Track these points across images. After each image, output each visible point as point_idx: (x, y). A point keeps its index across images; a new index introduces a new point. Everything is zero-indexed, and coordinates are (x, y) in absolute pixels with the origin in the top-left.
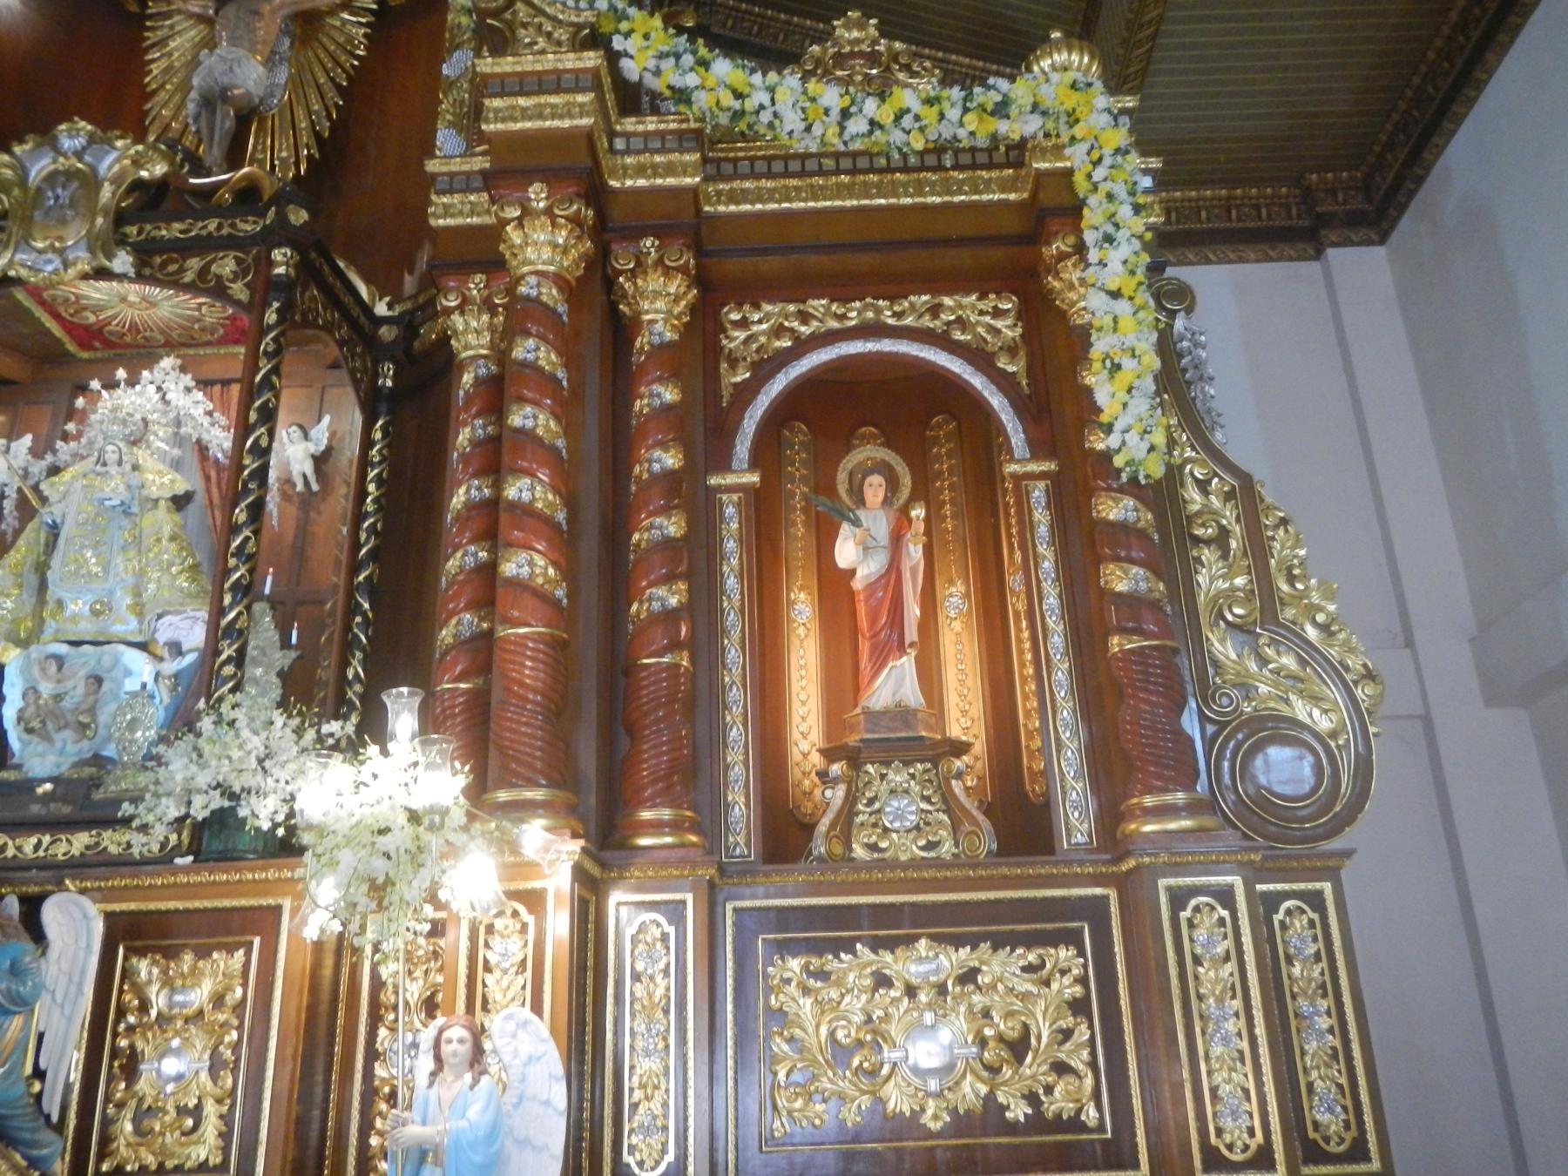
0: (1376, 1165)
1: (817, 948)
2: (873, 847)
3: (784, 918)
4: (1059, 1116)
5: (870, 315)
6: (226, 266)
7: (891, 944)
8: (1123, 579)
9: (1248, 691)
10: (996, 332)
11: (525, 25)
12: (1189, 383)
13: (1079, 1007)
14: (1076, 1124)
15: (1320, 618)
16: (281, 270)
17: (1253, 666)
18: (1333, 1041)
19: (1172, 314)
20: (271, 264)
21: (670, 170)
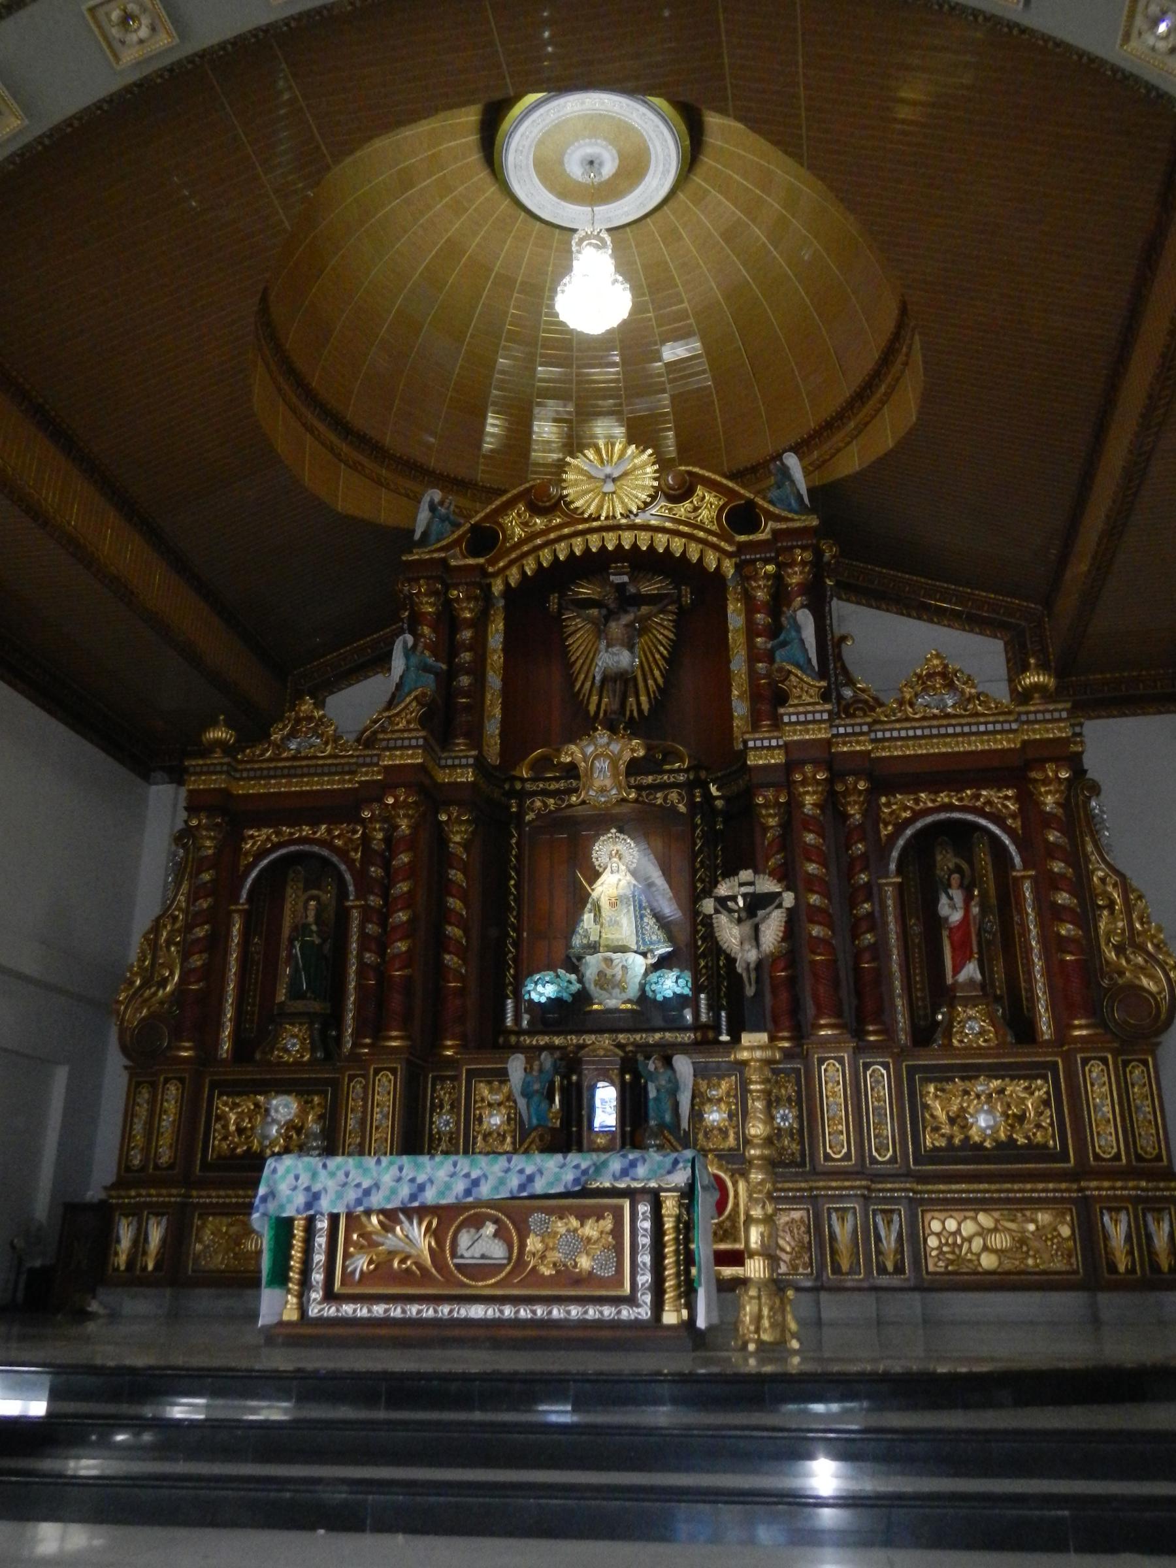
0: (1165, 1162)
1: (940, 1080)
2: (961, 1041)
3: (925, 1069)
4: (1038, 1144)
5: (946, 800)
6: (674, 796)
7: (969, 1078)
8: (1066, 929)
9: (1121, 973)
10: (1007, 807)
11: (795, 687)
12: (1097, 832)
13: (1046, 1103)
14: (1045, 1146)
15: (1155, 941)
16: (698, 800)
17: (1124, 963)
18: (1151, 1117)
19: (1089, 798)
20: (694, 796)
21: (858, 743)
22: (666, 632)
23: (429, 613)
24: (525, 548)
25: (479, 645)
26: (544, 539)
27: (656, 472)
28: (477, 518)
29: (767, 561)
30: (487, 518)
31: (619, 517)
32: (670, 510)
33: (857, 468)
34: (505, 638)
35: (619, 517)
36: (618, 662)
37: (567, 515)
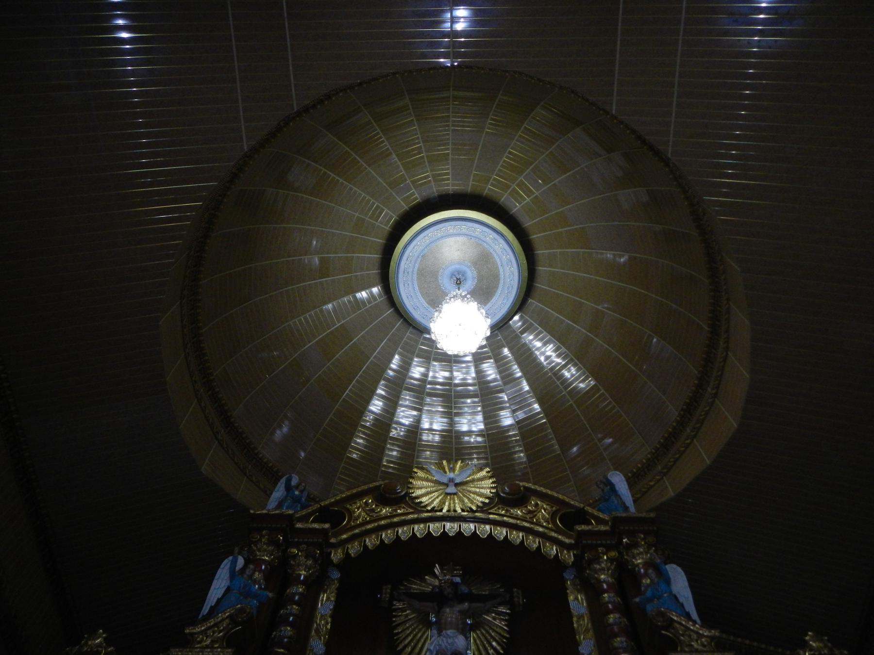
11: (683, 635)
22: (499, 630)
23: (265, 560)
24: (369, 527)
25: (309, 603)
26: (388, 521)
27: (493, 483)
28: (327, 503)
29: (609, 548)
30: (337, 503)
31: (459, 511)
32: (507, 511)
33: (671, 493)
34: (335, 606)
35: (459, 511)
36: (453, 644)
37: (411, 507)
